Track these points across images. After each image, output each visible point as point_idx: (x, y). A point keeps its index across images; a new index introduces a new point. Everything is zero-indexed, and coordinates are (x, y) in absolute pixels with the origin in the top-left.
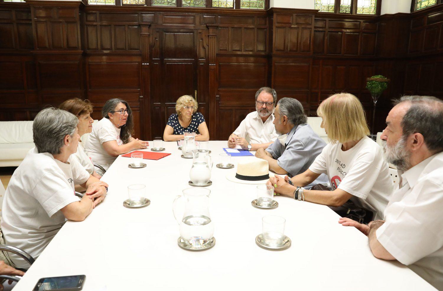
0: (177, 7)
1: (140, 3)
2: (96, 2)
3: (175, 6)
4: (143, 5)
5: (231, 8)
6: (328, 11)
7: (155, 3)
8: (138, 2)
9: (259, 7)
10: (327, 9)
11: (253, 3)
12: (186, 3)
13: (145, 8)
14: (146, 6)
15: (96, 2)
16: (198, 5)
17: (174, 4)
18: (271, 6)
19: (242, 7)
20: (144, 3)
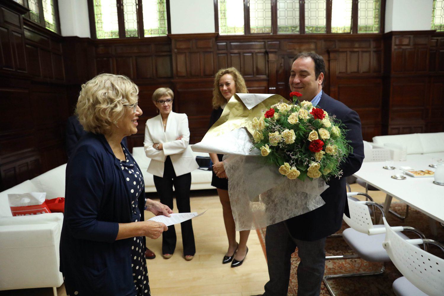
0: (301, 34)
1: (266, 32)
2: (227, 32)
3: (298, 33)
4: (269, 33)
5: (348, 33)
6: (441, 30)
7: (280, 32)
8: (265, 31)
9: (375, 31)
10: (440, 28)
11: (369, 27)
12: (309, 30)
13: (271, 36)
14: (272, 34)
15: (227, 32)
16: (319, 31)
17: (297, 31)
18: (387, 30)
19: (360, 32)
20: (270, 32)
